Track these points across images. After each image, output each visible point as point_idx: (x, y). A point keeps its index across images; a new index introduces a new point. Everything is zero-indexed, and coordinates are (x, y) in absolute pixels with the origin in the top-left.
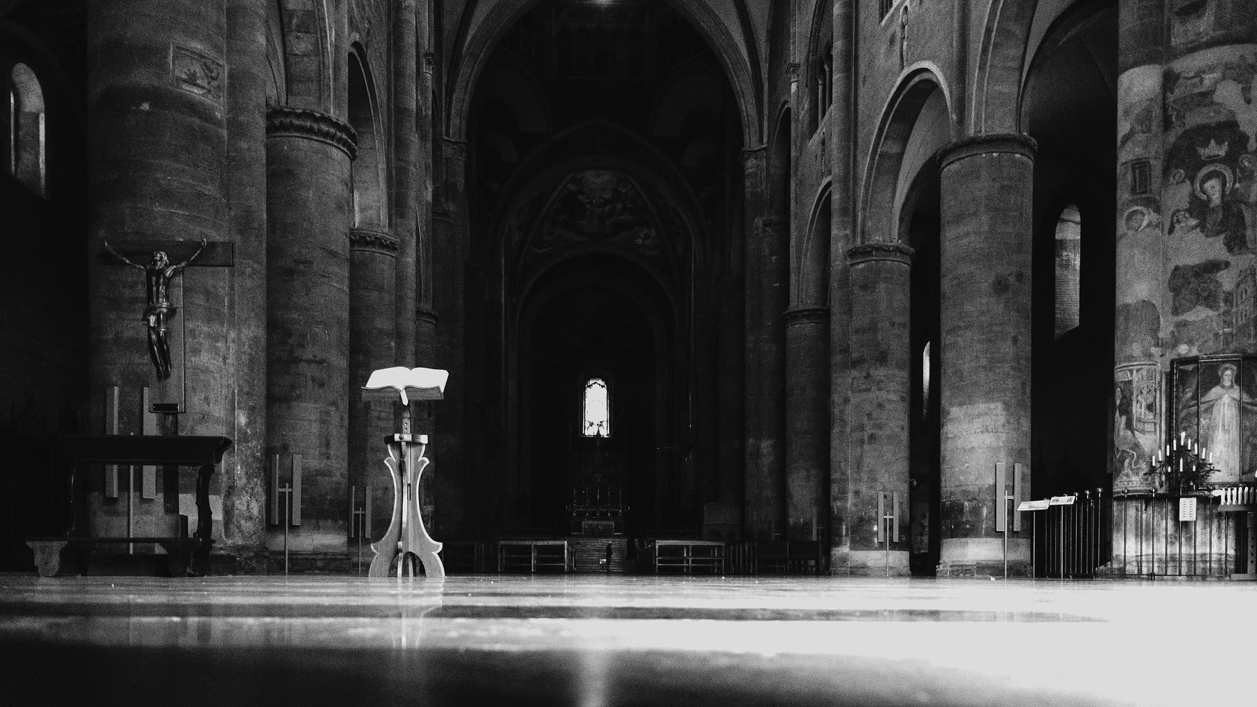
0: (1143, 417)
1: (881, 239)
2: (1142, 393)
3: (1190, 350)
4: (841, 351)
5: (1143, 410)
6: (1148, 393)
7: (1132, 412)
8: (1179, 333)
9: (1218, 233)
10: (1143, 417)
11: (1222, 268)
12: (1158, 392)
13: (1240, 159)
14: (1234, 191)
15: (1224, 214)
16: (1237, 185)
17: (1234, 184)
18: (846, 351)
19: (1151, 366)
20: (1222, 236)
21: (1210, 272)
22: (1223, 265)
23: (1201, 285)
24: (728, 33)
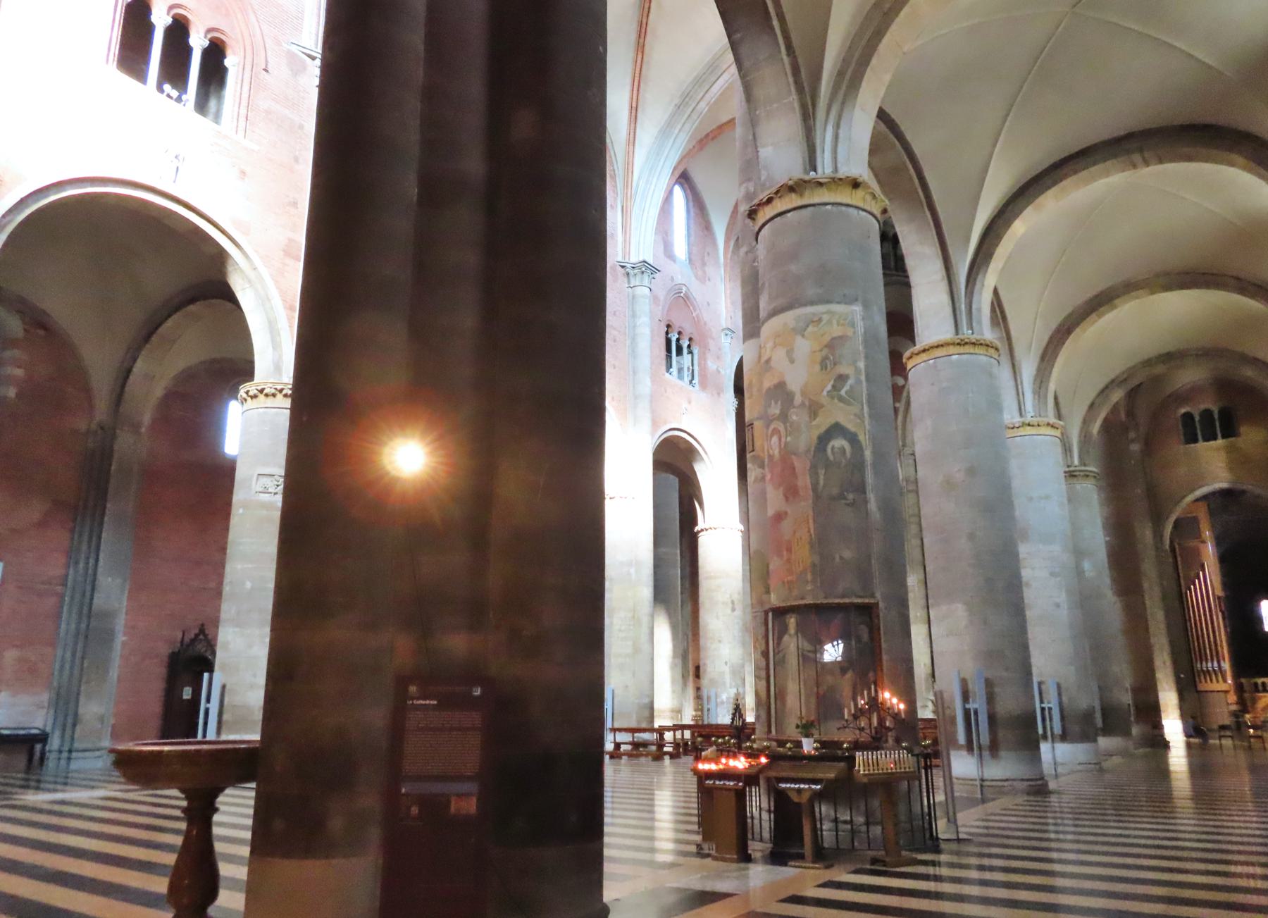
13: (789, 414)
16: (789, 439)
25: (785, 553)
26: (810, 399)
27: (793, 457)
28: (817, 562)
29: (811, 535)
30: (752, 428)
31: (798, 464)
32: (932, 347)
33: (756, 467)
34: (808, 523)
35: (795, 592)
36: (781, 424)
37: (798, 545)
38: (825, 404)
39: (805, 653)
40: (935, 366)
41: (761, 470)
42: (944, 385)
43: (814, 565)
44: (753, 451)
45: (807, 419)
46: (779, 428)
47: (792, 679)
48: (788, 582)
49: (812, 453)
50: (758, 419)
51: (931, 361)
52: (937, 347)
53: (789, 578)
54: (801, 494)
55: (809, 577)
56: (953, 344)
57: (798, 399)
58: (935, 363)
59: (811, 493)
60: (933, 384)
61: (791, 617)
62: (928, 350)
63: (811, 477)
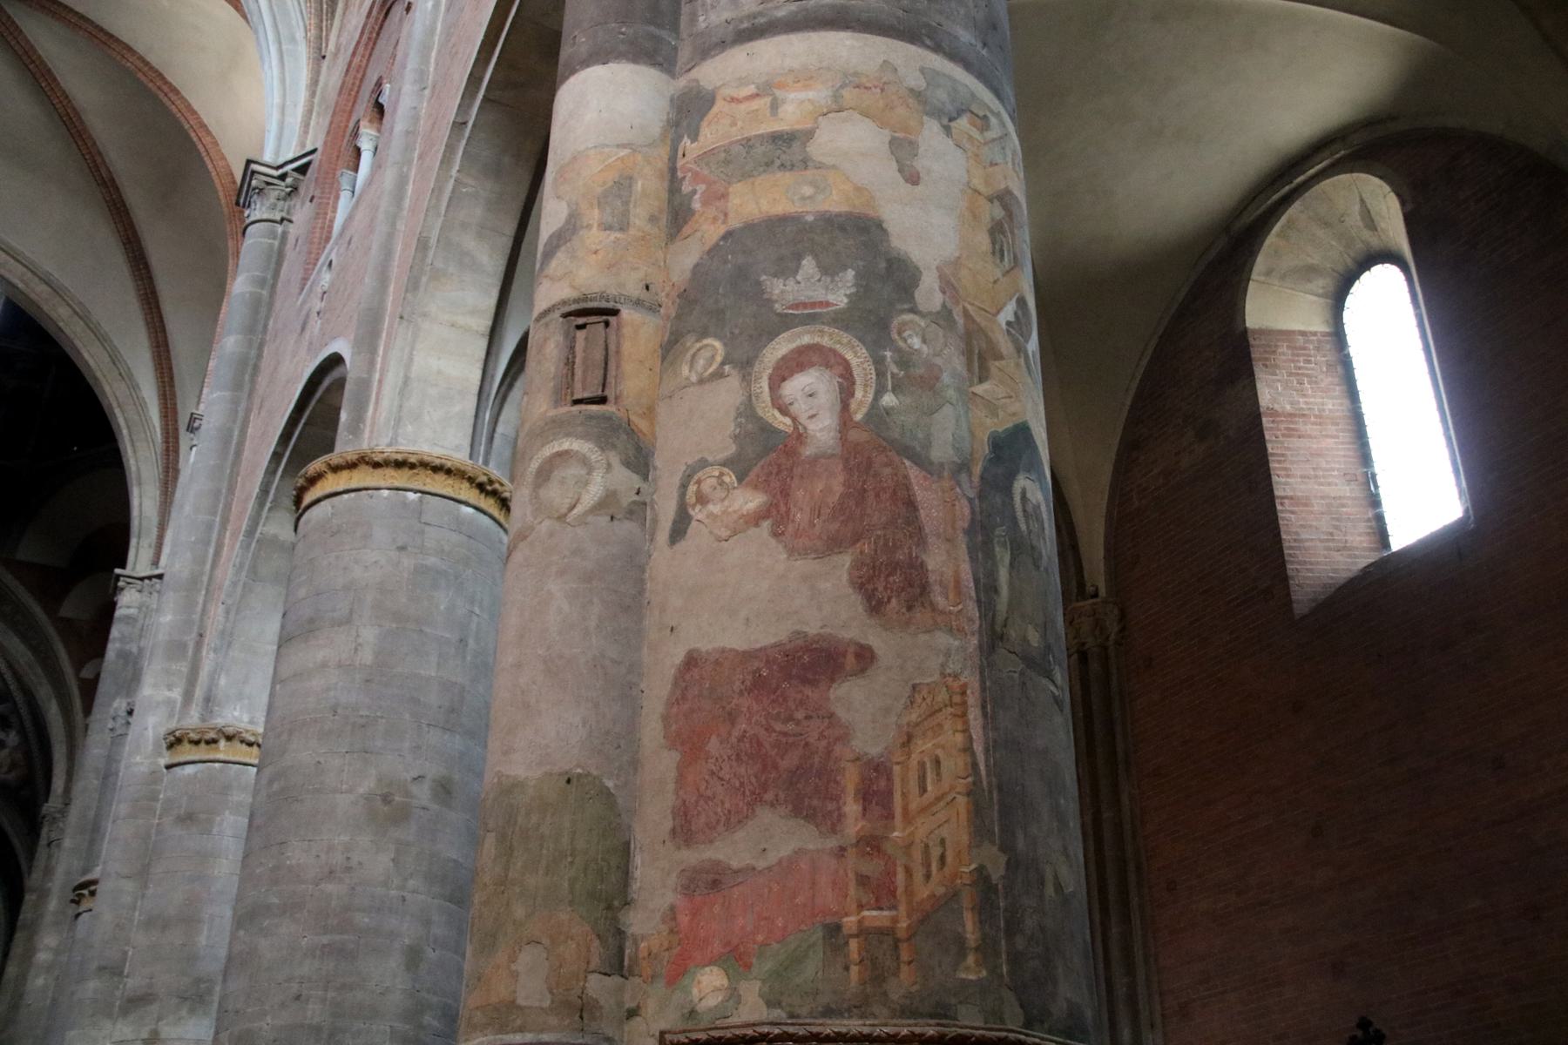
1: (246, 718)
3: (733, 995)
4: (101, 969)
8: (695, 913)
9: (834, 545)
11: (848, 668)
13: (895, 323)
14: (877, 415)
15: (847, 484)
17: (879, 393)
18: (114, 971)
20: (845, 560)
21: (805, 681)
22: (850, 661)
23: (779, 727)
24: (131, 376)
25: (852, 807)
26: (966, 313)
27: (914, 473)
28: (997, 873)
29: (975, 765)
31: (929, 498)
32: (424, 465)
33: (615, 459)
34: (964, 715)
35: (904, 983)
37: (923, 790)
38: (1005, 352)
40: (419, 511)
41: (636, 480)
42: (432, 560)
43: (981, 876)
44: (602, 400)
45: (958, 363)
46: (849, 356)
48: (863, 932)
49: (976, 479)
50: (638, 303)
51: (411, 495)
52: (437, 469)
53: (876, 917)
54: (940, 600)
55: (970, 928)
56: (471, 480)
57: (929, 294)
58: (421, 500)
59: (973, 610)
60: (402, 548)
62: (412, 466)
63: (973, 559)
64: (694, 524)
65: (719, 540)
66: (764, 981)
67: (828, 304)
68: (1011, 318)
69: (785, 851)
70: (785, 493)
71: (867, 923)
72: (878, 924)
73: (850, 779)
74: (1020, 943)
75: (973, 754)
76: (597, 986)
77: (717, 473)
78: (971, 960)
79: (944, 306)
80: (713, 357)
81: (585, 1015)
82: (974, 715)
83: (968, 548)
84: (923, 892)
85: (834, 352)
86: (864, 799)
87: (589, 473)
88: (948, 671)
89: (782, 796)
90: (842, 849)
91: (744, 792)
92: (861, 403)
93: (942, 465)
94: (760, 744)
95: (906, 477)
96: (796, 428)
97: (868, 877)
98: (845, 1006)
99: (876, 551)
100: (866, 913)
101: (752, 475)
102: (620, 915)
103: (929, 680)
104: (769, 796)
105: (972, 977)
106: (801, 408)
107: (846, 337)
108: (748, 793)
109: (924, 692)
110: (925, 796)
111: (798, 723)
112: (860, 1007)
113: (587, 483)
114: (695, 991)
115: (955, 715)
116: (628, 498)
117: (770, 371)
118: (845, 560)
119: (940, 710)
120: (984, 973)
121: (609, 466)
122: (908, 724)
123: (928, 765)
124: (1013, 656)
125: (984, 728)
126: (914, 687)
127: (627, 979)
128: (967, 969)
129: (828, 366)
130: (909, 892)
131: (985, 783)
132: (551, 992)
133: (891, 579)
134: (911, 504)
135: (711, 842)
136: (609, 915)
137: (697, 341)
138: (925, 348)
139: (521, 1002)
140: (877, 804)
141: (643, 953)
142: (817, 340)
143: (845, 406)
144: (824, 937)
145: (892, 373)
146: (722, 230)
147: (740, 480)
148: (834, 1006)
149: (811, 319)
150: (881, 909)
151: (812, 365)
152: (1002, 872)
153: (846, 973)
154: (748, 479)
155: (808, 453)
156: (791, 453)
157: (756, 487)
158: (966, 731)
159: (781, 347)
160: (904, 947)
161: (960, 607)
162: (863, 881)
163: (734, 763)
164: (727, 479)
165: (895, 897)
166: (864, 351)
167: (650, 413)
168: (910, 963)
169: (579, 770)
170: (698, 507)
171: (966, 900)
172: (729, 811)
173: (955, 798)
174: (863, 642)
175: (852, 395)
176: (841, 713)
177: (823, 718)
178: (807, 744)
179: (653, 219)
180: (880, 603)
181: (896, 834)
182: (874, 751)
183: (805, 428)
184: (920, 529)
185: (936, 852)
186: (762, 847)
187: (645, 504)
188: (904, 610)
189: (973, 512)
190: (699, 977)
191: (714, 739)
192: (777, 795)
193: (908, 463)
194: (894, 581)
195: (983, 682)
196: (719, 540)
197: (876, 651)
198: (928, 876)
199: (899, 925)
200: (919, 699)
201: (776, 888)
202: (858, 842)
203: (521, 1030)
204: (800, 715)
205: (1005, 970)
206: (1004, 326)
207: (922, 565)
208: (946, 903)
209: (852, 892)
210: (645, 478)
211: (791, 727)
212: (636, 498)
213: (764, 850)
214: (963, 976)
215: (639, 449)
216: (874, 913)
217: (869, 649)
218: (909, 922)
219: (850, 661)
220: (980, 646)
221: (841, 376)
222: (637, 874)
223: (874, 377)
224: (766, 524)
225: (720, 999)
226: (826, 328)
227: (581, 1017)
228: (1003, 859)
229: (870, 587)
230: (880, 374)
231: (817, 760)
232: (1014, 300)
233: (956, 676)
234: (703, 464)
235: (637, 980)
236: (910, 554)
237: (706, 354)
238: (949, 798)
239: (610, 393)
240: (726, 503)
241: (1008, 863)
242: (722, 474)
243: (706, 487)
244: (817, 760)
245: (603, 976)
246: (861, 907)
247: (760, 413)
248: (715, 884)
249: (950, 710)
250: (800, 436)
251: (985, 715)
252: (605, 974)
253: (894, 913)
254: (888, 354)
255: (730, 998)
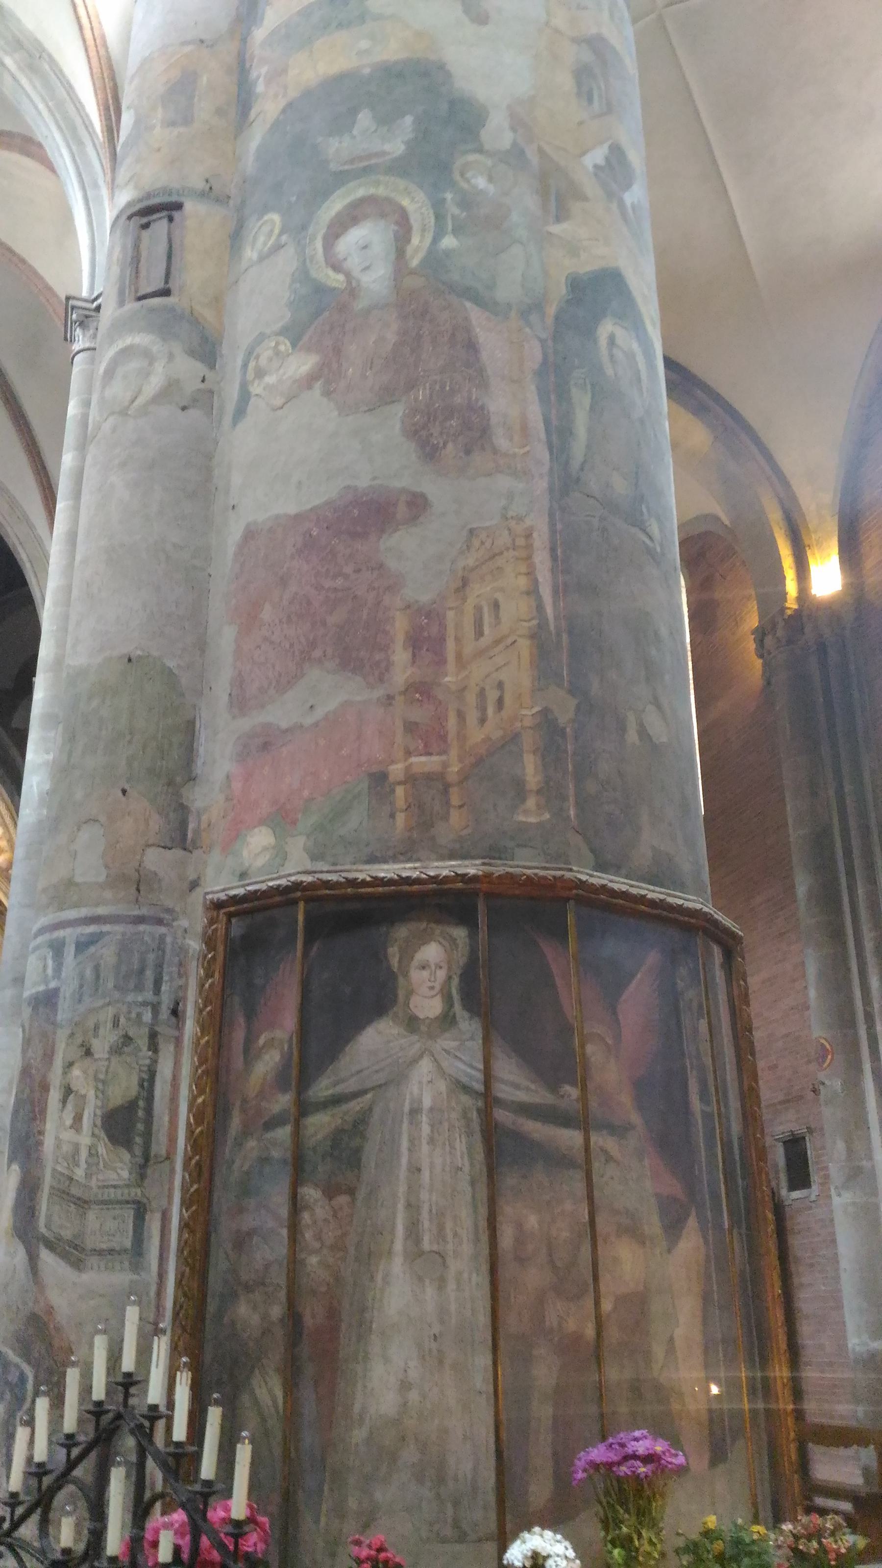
0: (79, 1173)
2: (88, 1053)
3: (280, 854)
5: (85, 1140)
6: (116, 1050)
7: (40, 1143)
10: (79, 1173)
12: (167, 1051)
13: (459, 162)
19: (142, 928)
20: (399, 410)
23: (328, 584)
25: (400, 656)
27: (475, 315)
28: (565, 713)
29: (540, 608)
30: (171, 219)
33: (177, 348)
34: (529, 558)
36: (421, 196)
37: (479, 633)
39: (501, 1115)
41: (200, 368)
44: (165, 292)
45: (531, 202)
46: (405, 202)
47: (415, 1254)
48: (410, 779)
49: (550, 321)
53: (422, 763)
54: (501, 442)
61: (424, 939)
64: (253, 400)
65: (275, 409)
66: (308, 836)
67: (383, 153)
68: (601, 161)
69: (332, 705)
70: (338, 351)
71: (415, 770)
72: (426, 769)
73: (400, 626)
74: (591, 787)
75: (539, 598)
76: (154, 860)
77: (273, 344)
78: (531, 802)
79: (515, 144)
80: (272, 231)
81: (141, 888)
82: (542, 559)
83: (538, 389)
84: (476, 735)
85: (388, 200)
86: (414, 648)
87: (151, 364)
88: (510, 514)
89: (329, 652)
90: (390, 698)
91: (294, 652)
92: (417, 250)
93: (509, 306)
94: (309, 603)
95: (466, 319)
96: (349, 282)
97: (416, 724)
98: (390, 853)
99: (431, 395)
100: (414, 759)
101: (306, 338)
102: (184, 791)
103: (487, 524)
104: (317, 653)
105: (532, 820)
106: (354, 263)
107: (402, 183)
108: (297, 653)
109: (483, 536)
110: (482, 639)
111: (346, 577)
112: (405, 853)
113: (148, 374)
114: (245, 853)
115: (517, 559)
116: (192, 386)
117: (324, 231)
118: (399, 410)
119: (501, 553)
120: (547, 816)
121: (171, 357)
122: (464, 568)
123: (486, 609)
124: (592, 501)
125: (553, 571)
126: (471, 531)
127: (191, 852)
128: (526, 812)
129: (383, 215)
130: (462, 737)
131: (552, 627)
132: (107, 867)
133: (448, 424)
134: (472, 346)
135: (263, 706)
136: (170, 790)
137: (258, 219)
138: (491, 189)
139: (78, 879)
140: (427, 650)
141: (204, 825)
142: (372, 191)
143: (400, 253)
144: (369, 788)
145: (453, 216)
146: (282, 103)
147: (294, 345)
148: (378, 855)
149: (367, 171)
150: (430, 754)
151: (366, 217)
152: (571, 714)
153: (391, 820)
154: (301, 343)
155: (360, 306)
156: (343, 308)
157: (309, 350)
158: (531, 574)
159: (336, 205)
160: (454, 792)
161: (527, 449)
162: (411, 728)
163: (285, 626)
164: (282, 348)
165: (445, 741)
166: (422, 195)
167: (217, 301)
168: (461, 807)
169: (139, 652)
170: (256, 382)
171: (528, 741)
172: (280, 675)
173: (515, 641)
174: (418, 490)
175: (409, 241)
176: (392, 564)
177: (372, 569)
178: (355, 597)
179: (220, 112)
180: (435, 448)
181: (447, 679)
182: (425, 598)
183: (358, 281)
184: (481, 371)
185: (492, 696)
186: (310, 705)
187: (211, 392)
188: (462, 454)
189: (545, 356)
190: (249, 839)
191: (268, 607)
192: (324, 652)
193: (468, 304)
194: (451, 425)
195: (552, 525)
196: (275, 409)
197: (430, 497)
198: (483, 720)
199: (449, 770)
200: (476, 543)
201: (322, 742)
202: (407, 690)
203: (76, 906)
204: (348, 569)
205: (572, 813)
206: (591, 169)
207: (482, 408)
208: (503, 746)
209: (399, 738)
210: (212, 366)
211: (339, 582)
212: (202, 386)
213: (312, 707)
214: (522, 818)
215: (205, 339)
216: (423, 759)
217: (423, 496)
218: (460, 765)
219: (402, 510)
220: (551, 490)
221: (397, 223)
222: (201, 750)
223: (433, 220)
224: (318, 385)
225: (268, 857)
226: (382, 178)
227: (138, 890)
228: (572, 703)
229: (424, 433)
230: (439, 217)
231: (365, 612)
232: (606, 147)
233: (520, 519)
234: (261, 338)
235: (200, 851)
236: (470, 399)
237: (266, 229)
238: (509, 641)
239: (173, 285)
240: (281, 371)
241: (578, 708)
242: (277, 344)
243: (263, 361)
244: (365, 612)
245: (162, 850)
246: (408, 753)
247: (314, 274)
248: (266, 746)
249: (512, 553)
250: (353, 290)
251: (554, 558)
252: (164, 847)
253: (444, 758)
254: (449, 196)
255: (277, 856)
